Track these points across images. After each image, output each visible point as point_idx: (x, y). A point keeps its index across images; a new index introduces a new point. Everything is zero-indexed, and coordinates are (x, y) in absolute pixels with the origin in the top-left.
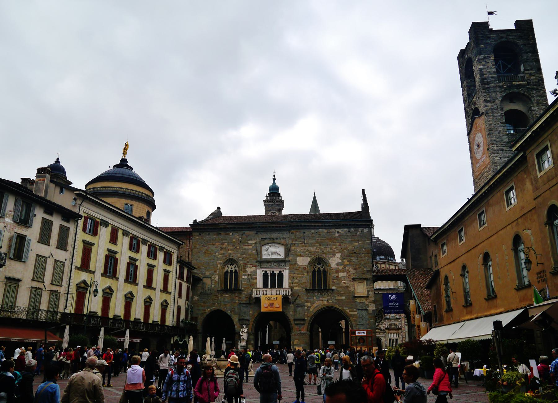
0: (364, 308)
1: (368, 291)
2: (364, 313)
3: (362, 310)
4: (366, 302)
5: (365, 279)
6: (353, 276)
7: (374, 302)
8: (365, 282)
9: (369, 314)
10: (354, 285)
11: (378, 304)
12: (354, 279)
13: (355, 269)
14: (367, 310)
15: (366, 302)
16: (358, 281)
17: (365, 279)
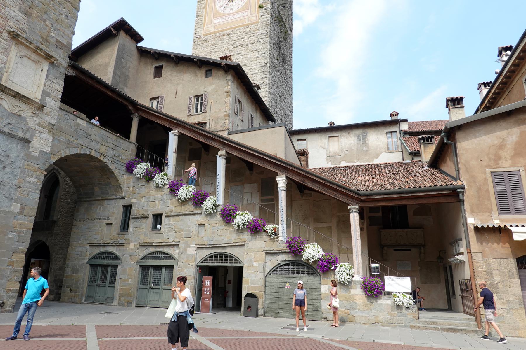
0: (20, 134)
1: (45, 94)
2: (15, 149)
3: (11, 136)
4: (33, 122)
5: (48, 57)
6: (12, 25)
7: (52, 129)
8: (46, 66)
9: (28, 157)
10: (7, 52)
11: (62, 138)
12: (15, 37)
13: (27, 14)
14: (27, 142)
15: (33, 122)
16: (25, 52)
17: (48, 57)
